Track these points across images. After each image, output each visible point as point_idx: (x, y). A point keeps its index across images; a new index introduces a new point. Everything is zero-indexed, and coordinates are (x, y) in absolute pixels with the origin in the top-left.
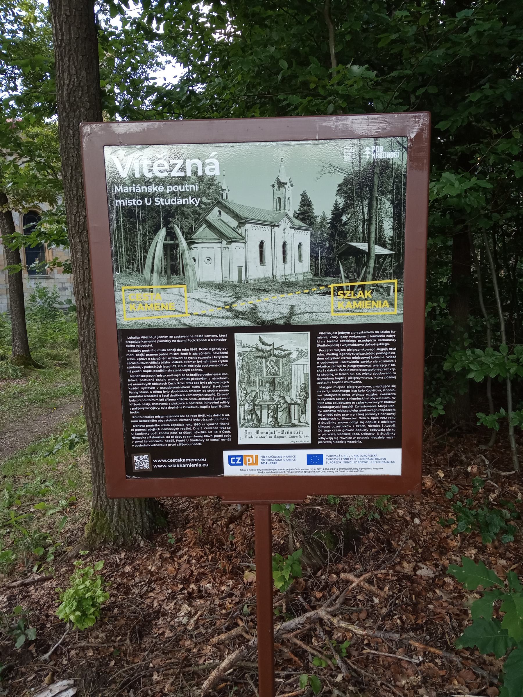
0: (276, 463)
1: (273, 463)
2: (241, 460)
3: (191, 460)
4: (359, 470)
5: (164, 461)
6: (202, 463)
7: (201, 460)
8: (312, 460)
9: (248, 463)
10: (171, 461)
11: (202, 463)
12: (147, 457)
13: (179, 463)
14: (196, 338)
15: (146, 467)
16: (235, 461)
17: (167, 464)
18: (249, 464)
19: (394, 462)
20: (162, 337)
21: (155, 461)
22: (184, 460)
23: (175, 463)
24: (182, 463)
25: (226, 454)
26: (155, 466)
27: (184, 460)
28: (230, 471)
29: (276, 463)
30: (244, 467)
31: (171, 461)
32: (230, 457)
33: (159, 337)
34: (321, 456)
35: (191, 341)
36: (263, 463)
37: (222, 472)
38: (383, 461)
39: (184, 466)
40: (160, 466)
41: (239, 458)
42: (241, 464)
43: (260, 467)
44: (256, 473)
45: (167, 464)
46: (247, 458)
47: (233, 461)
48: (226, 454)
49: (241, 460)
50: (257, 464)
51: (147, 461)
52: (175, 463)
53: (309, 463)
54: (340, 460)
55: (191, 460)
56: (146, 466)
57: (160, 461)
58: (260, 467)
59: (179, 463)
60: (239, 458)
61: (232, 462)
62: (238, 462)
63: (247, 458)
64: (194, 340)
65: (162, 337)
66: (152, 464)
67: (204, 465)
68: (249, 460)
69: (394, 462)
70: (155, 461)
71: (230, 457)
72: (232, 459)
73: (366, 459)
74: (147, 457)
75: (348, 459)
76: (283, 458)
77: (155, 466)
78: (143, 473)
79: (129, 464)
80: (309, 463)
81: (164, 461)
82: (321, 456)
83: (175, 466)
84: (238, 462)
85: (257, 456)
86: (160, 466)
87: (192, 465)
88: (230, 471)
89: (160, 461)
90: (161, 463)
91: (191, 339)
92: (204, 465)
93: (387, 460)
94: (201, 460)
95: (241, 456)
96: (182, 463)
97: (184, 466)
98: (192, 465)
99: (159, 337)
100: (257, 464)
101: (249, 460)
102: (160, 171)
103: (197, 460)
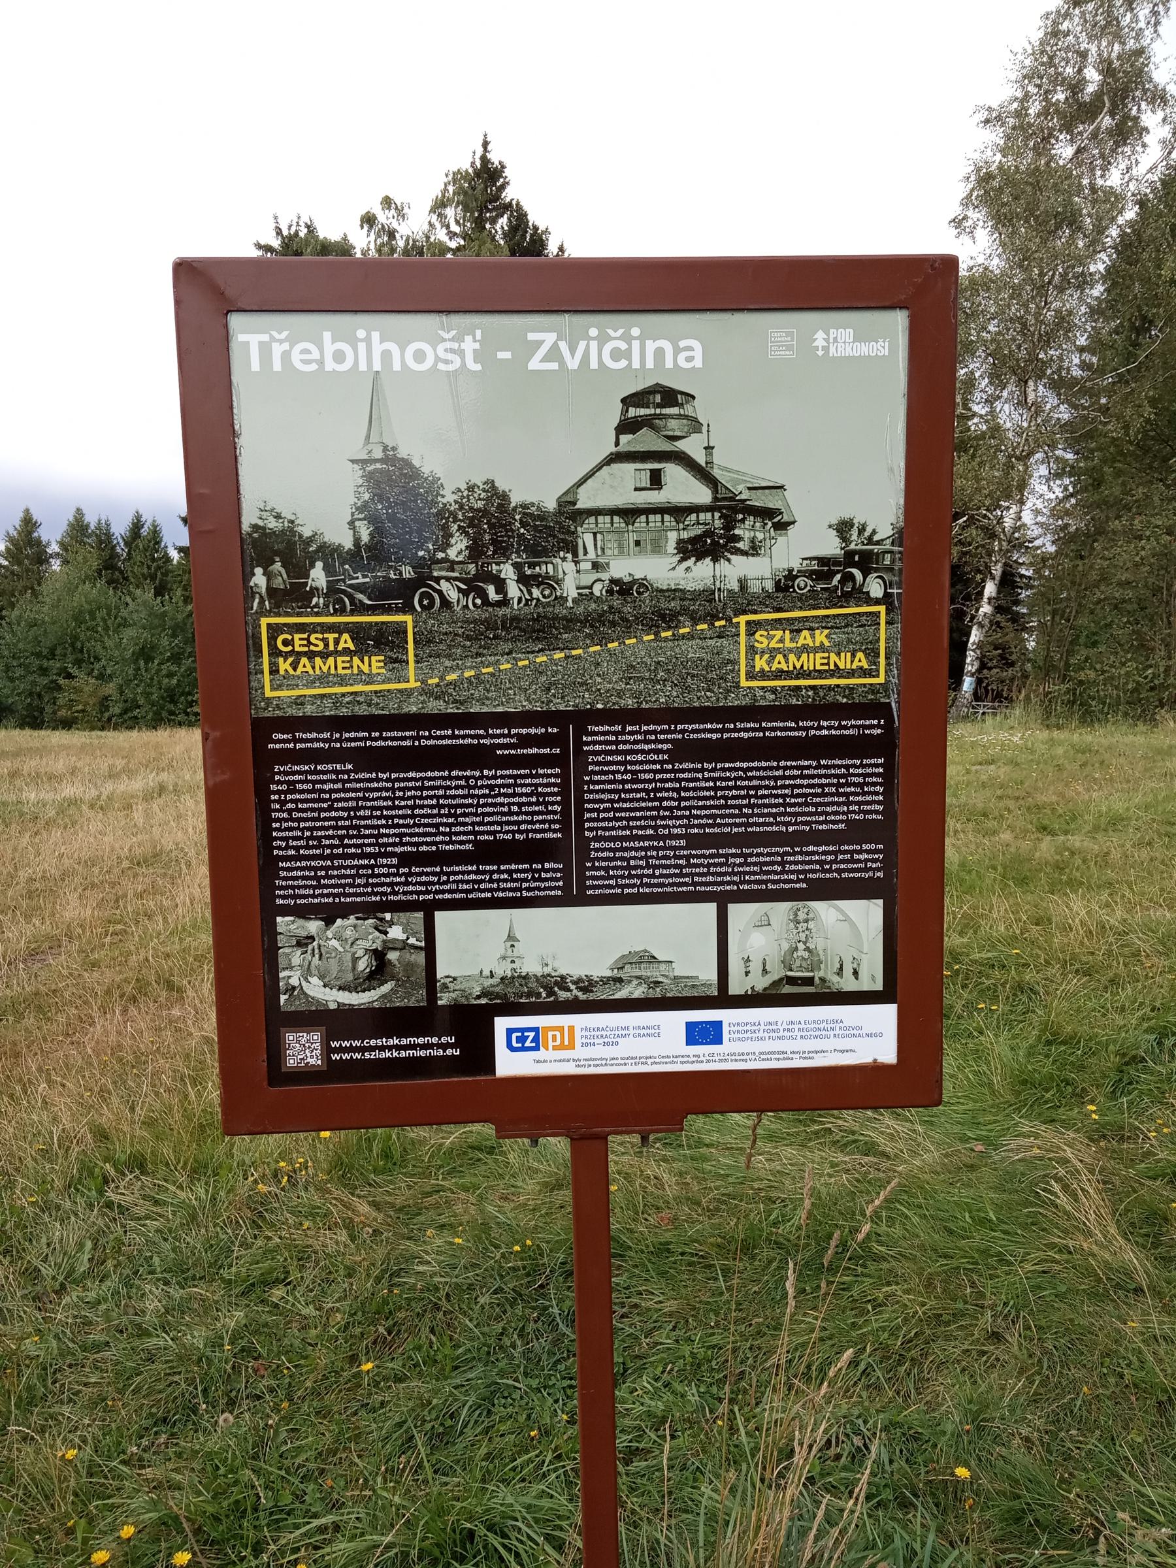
0: (617, 1043)
1: (608, 1044)
2: (536, 1039)
3: (420, 1041)
4: (803, 1055)
5: (356, 1043)
6: (445, 1047)
7: (444, 1040)
8: (699, 1034)
9: (551, 1044)
10: (373, 1043)
11: (445, 1047)
12: (316, 1036)
13: (390, 1048)
14: (386, 739)
15: (312, 1061)
16: (522, 1039)
17: (362, 1050)
18: (555, 1048)
19: (880, 1035)
20: (353, 735)
21: (335, 1044)
22: (404, 1041)
23: (382, 1048)
24: (399, 1048)
25: (502, 1024)
26: (335, 1057)
27: (404, 1041)
28: (509, 1064)
29: (617, 1043)
30: (541, 1054)
31: (373, 1043)
32: (510, 1032)
33: (346, 735)
34: (718, 1025)
35: (374, 744)
36: (587, 1045)
37: (491, 1068)
38: (855, 1032)
39: (403, 1054)
40: (346, 1056)
41: (532, 1035)
42: (537, 1048)
43: (580, 1052)
44: (569, 1069)
45: (362, 1050)
46: (550, 1034)
47: (519, 1040)
48: (502, 1024)
49: (536, 1039)
50: (571, 1046)
51: (317, 1045)
52: (382, 1048)
53: (691, 1041)
54: (761, 1034)
55: (420, 1041)
56: (314, 1059)
57: (346, 1044)
58: (580, 1052)
59: (390, 1048)
60: (532, 1035)
61: (515, 1044)
62: (528, 1044)
63: (550, 1034)
64: (381, 743)
65: (353, 735)
66: (327, 1050)
67: (449, 1052)
68: (554, 1037)
69: (880, 1035)
70: (335, 1044)
71: (510, 1032)
72: (514, 1035)
73: (817, 1030)
74: (316, 1036)
75: (778, 1031)
76: (632, 1032)
77: (335, 1057)
78: (305, 1075)
79: (276, 1051)
80: (691, 1041)
81: (356, 1043)
82: (718, 1025)
83: (383, 1055)
84: (528, 1044)
85: (571, 1029)
86: (346, 1056)
87: (423, 1053)
88: (509, 1064)
89: (346, 1044)
90: (349, 1050)
91: (376, 739)
92: (449, 1052)
93: (864, 1032)
94: (444, 1040)
95: (536, 1030)
96: (399, 1048)
97: (403, 1054)
98: (423, 1053)
99: (346, 735)
100: (571, 1046)
101: (554, 1037)
102: (304, 362)
103: (435, 1040)
